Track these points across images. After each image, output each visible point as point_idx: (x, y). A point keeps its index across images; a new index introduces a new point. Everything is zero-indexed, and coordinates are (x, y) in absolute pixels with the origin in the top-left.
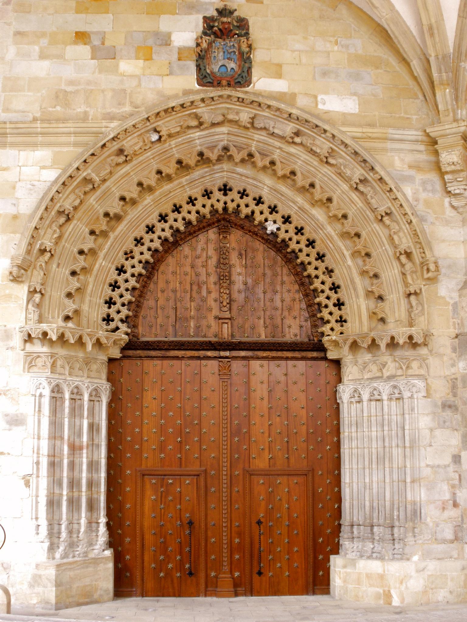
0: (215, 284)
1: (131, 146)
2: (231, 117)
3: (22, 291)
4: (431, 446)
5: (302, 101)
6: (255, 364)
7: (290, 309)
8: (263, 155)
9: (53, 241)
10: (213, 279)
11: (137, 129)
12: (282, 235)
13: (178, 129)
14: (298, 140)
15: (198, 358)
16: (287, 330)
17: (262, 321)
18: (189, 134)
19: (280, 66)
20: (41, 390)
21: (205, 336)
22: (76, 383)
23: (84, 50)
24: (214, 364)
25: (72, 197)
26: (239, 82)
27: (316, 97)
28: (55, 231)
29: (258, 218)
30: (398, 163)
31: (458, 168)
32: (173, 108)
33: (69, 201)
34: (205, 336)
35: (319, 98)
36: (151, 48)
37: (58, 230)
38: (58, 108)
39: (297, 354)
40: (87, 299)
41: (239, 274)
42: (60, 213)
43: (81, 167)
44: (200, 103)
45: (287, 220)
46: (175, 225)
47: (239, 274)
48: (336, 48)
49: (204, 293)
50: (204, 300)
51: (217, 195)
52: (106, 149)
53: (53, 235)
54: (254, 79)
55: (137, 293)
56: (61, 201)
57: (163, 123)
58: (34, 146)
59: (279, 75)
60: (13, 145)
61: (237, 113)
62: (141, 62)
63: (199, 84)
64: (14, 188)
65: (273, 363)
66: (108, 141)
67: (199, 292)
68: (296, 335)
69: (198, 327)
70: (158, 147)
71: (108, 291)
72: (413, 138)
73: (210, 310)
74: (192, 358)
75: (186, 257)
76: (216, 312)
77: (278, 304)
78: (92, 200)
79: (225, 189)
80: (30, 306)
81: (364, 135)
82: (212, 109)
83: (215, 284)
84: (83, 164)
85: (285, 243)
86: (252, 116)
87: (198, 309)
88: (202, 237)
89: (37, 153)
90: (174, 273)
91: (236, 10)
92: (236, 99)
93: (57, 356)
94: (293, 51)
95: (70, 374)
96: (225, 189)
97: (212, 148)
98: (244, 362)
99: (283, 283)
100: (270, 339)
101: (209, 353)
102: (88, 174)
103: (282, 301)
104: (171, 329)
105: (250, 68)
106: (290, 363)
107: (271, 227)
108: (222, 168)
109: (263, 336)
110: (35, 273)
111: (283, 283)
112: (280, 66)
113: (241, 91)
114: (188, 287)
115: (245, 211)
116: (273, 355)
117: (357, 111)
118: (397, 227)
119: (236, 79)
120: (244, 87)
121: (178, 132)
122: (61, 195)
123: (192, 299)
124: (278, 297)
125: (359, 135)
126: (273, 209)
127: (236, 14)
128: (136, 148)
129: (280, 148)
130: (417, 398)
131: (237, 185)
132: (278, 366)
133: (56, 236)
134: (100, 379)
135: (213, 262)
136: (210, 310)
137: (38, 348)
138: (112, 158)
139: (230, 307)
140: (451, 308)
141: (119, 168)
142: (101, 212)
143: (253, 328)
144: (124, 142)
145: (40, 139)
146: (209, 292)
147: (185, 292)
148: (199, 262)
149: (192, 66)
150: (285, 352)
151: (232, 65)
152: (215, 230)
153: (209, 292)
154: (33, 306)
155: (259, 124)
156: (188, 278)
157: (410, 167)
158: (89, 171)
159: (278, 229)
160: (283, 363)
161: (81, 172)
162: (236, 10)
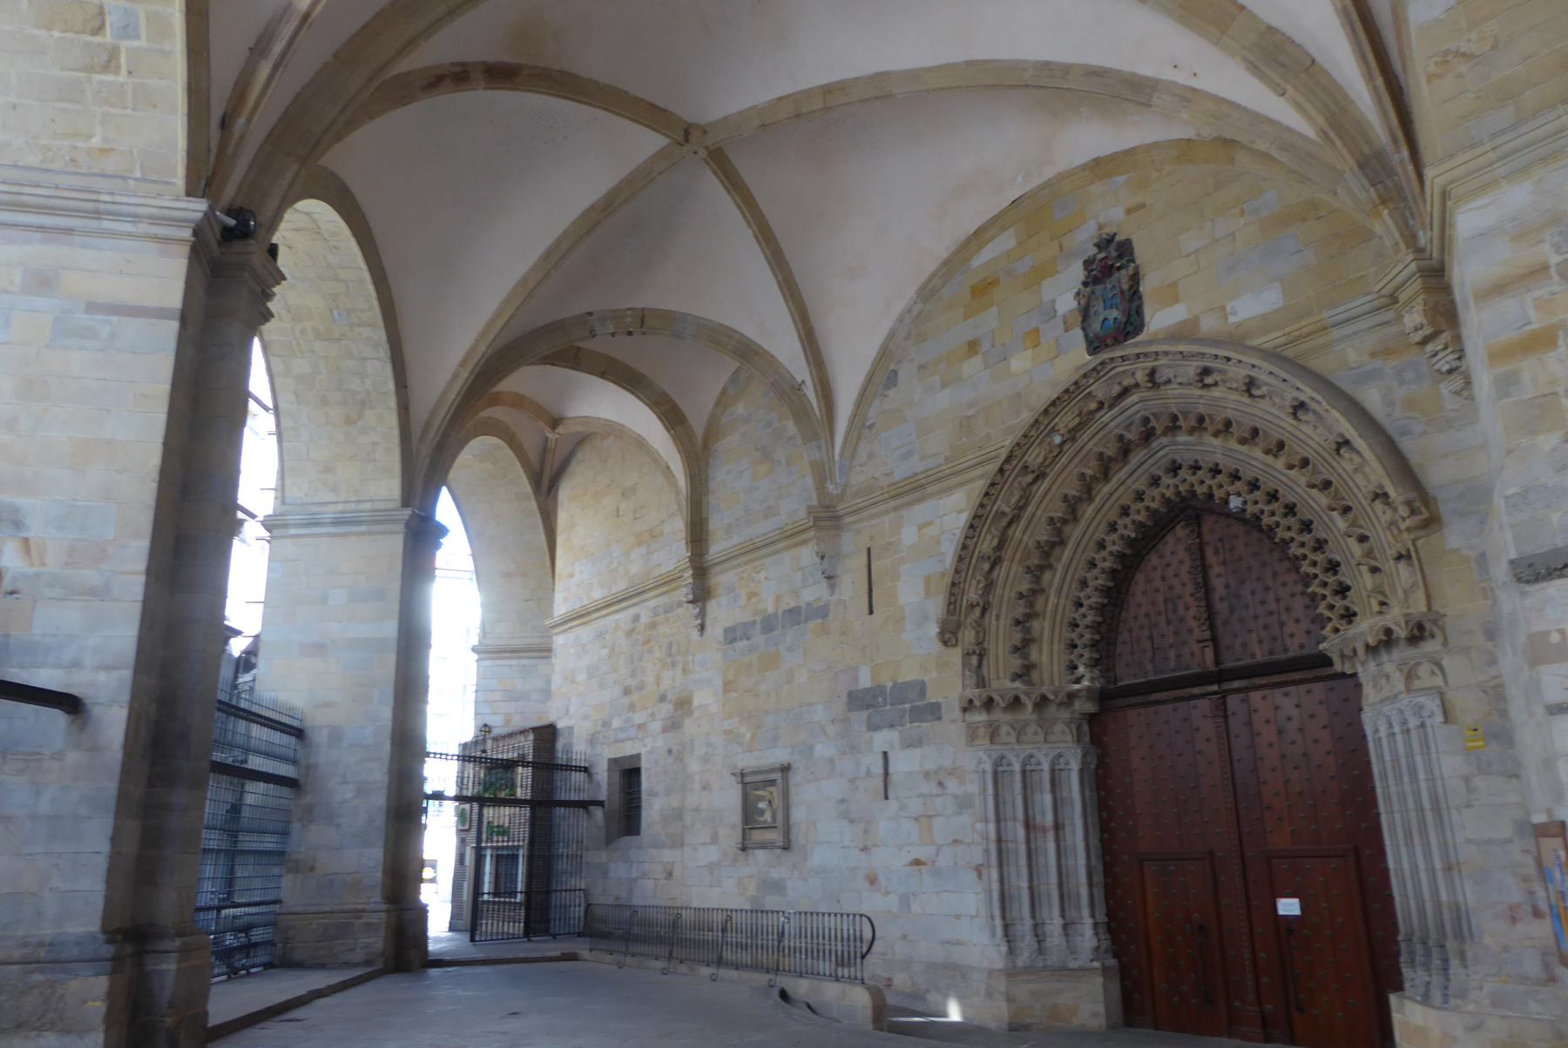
0: (1192, 595)
1: (1034, 460)
2: (1126, 383)
3: (956, 655)
4: (1469, 806)
5: (1208, 325)
6: (1256, 696)
7: (1288, 609)
8: (1186, 414)
9: (980, 592)
10: (1189, 589)
11: (1033, 438)
12: (1250, 509)
13: (1077, 420)
14: (1209, 380)
15: (1183, 699)
16: (1288, 642)
17: (1254, 636)
18: (1099, 420)
19: (1174, 285)
20: (982, 766)
21: (1187, 668)
22: (1028, 752)
23: (976, 362)
24: (1204, 704)
25: (989, 537)
26: (1128, 333)
27: (1223, 308)
28: (979, 581)
29: (1218, 494)
30: (1353, 356)
31: (1428, 331)
32: (1058, 398)
33: (986, 543)
34: (1187, 668)
35: (1228, 310)
36: (1037, 330)
37: (983, 579)
38: (964, 439)
39: (1308, 674)
40: (1045, 647)
41: (1219, 576)
42: (982, 558)
43: (985, 502)
44: (1085, 381)
45: (1254, 485)
46: (1126, 532)
47: (1219, 576)
48: (1242, 221)
49: (1181, 610)
50: (1182, 620)
51: (1167, 480)
52: (1007, 474)
53: (978, 586)
54: (1147, 319)
55: (1103, 629)
56: (979, 544)
57: (1060, 420)
58: (948, 490)
59: (1175, 300)
60: (932, 495)
61: (1133, 374)
62: (1030, 351)
63: (1090, 355)
64: (939, 543)
65: (1278, 692)
66: (1003, 464)
67: (1175, 611)
68: (1302, 646)
69: (1179, 656)
70: (1070, 449)
71: (1070, 635)
72: (1367, 308)
73: (1191, 631)
74: (1176, 700)
75: (1155, 568)
76: (1197, 634)
77: (1272, 606)
78: (1017, 532)
79: (1174, 469)
80: (967, 673)
81: (1290, 338)
82: (1105, 381)
83: (1192, 595)
84: (986, 498)
85: (1257, 518)
86: (1147, 372)
87: (1176, 633)
88: (1170, 538)
89: (953, 496)
90: (1145, 593)
91: (1115, 234)
92: (1120, 360)
93: (997, 723)
94: (1187, 256)
95: (1018, 741)
96: (1174, 469)
97: (1128, 428)
98: (1242, 696)
99: (1275, 574)
100: (1268, 658)
101: (1196, 691)
102: (999, 507)
103: (1278, 600)
104: (1149, 667)
105: (1139, 311)
106: (1303, 688)
107: (1235, 503)
108: (1161, 443)
109: (1260, 655)
110: (966, 632)
111: (1275, 574)
112: (1174, 285)
113: (1130, 344)
114: (1162, 608)
115: (1200, 490)
116: (1276, 680)
117: (1281, 303)
118: (1359, 460)
119: (1124, 328)
120: (1137, 335)
121: (1080, 424)
122: (975, 540)
123: (1169, 622)
124: (1271, 596)
125: (1283, 340)
126: (1235, 477)
127: (1117, 238)
128: (1040, 460)
129: (1201, 397)
130: (1432, 727)
131: (1185, 457)
132: (1286, 694)
133: (981, 585)
134: (1066, 742)
135: (1186, 567)
136: (1191, 631)
137: (979, 717)
138: (1019, 479)
139: (1210, 624)
140: (1473, 565)
141: (1035, 487)
142: (1031, 544)
143: (1244, 645)
144: (1024, 459)
145: (954, 481)
146: (1187, 608)
147: (1160, 613)
148: (1170, 571)
149: (1077, 334)
150: (1290, 674)
151: (1114, 314)
152: (1182, 524)
153: (1187, 608)
154: (970, 671)
155: (1160, 378)
156: (1161, 597)
157: (1373, 355)
158: (999, 502)
159: (1245, 502)
160: (1292, 689)
161: (988, 508)
162: (1115, 234)
